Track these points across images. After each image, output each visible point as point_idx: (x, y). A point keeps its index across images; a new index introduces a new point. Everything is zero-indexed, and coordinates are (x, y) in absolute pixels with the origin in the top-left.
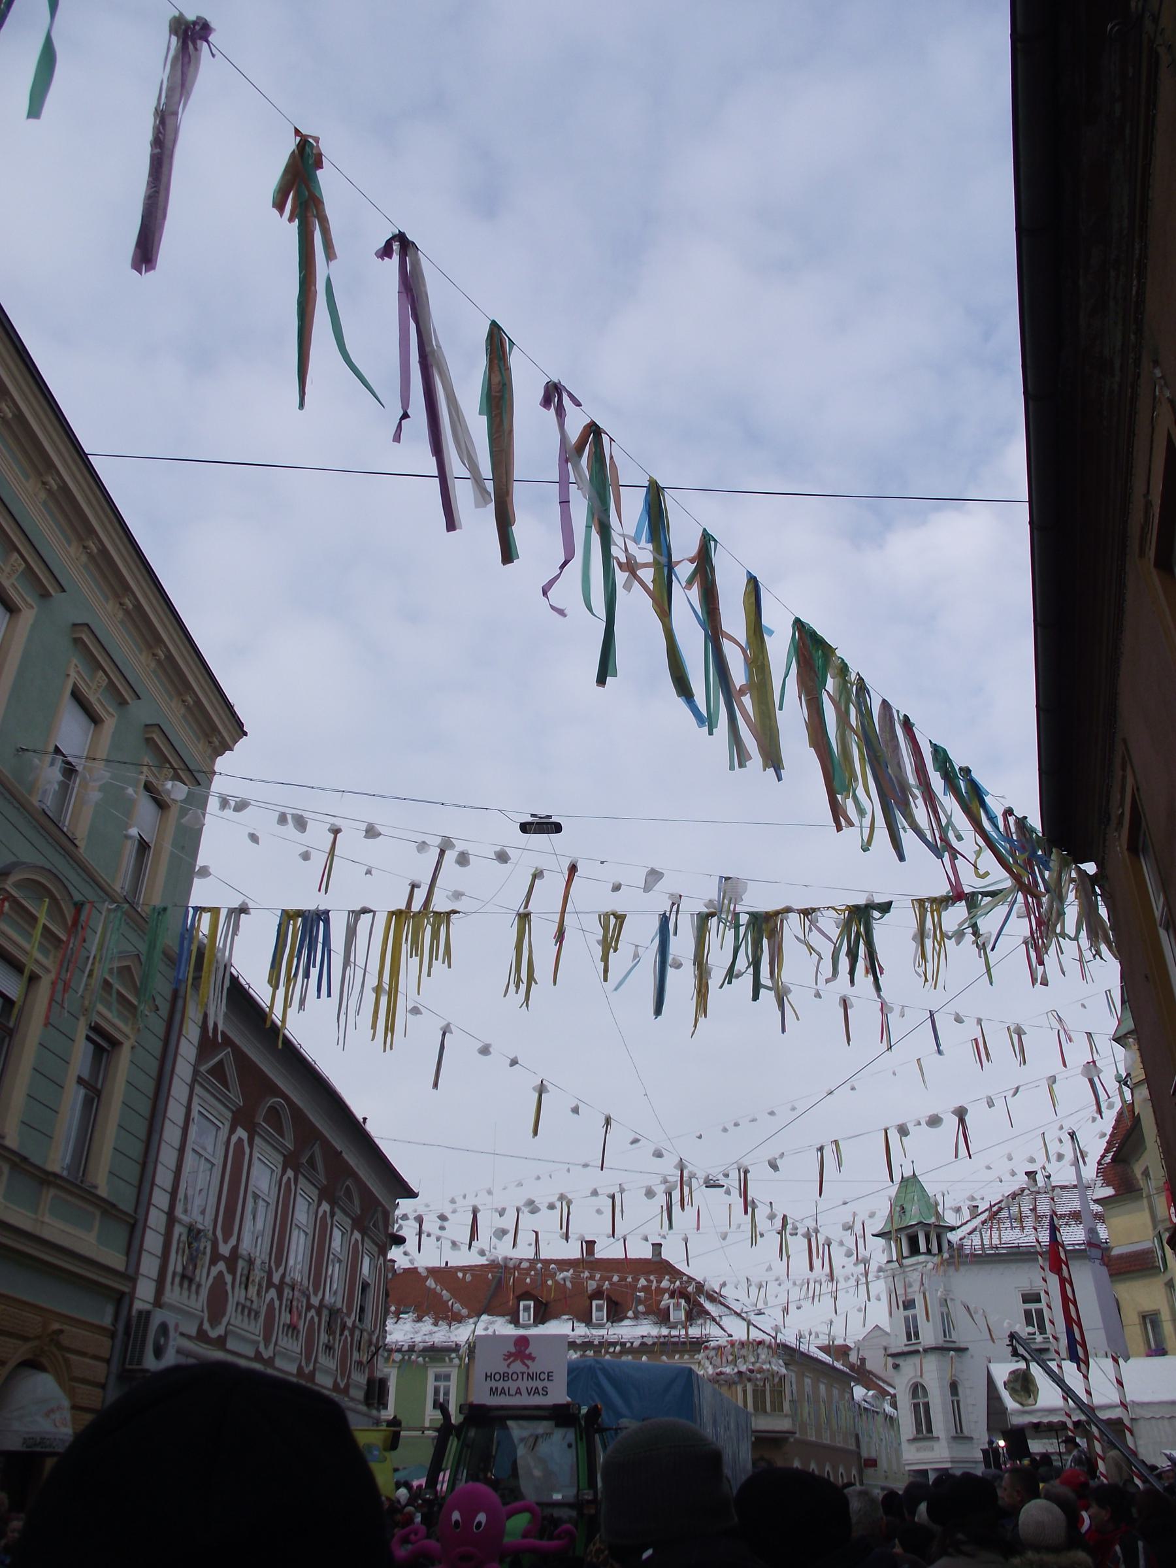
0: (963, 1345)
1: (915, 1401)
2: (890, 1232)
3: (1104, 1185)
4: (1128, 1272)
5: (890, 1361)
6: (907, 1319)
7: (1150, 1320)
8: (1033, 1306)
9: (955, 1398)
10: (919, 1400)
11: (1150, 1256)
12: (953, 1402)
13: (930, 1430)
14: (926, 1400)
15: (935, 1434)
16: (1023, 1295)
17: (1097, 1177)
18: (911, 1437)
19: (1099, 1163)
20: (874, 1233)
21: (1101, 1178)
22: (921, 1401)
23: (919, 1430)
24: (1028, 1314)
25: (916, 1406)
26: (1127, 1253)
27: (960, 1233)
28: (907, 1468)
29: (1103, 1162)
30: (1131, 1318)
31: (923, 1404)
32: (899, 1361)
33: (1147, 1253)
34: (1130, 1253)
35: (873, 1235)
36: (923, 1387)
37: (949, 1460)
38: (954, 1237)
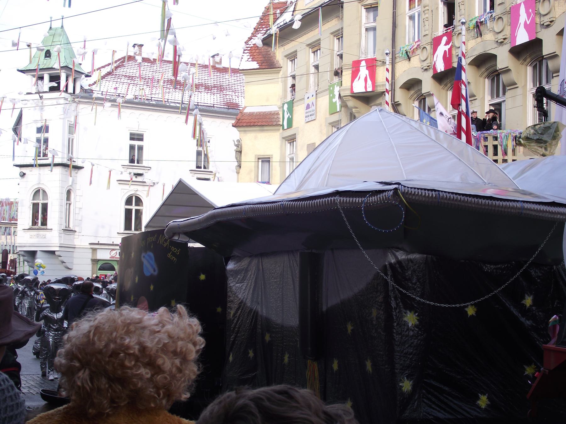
0: (79, 163)
1: (35, 202)
2: (36, 69)
3: (250, 60)
4: (254, 126)
5: (18, 170)
6: (38, 141)
7: (266, 160)
8: (136, 143)
9: (68, 202)
10: (38, 201)
11: (276, 117)
12: (67, 204)
13: (44, 223)
14: (45, 202)
15: (49, 226)
16: (131, 134)
17: (244, 53)
18: (28, 227)
19: (246, 43)
20: (20, 69)
21: (248, 54)
22: (41, 202)
23: (34, 223)
24: (132, 148)
25: (35, 206)
26: (257, 113)
27: (91, 80)
28: (19, 249)
29: (250, 43)
30: (249, 158)
31: (42, 204)
32: (24, 170)
33: (273, 114)
34: (260, 113)
35: (18, 70)
36: (44, 192)
37: (59, 245)
38: (84, 82)
